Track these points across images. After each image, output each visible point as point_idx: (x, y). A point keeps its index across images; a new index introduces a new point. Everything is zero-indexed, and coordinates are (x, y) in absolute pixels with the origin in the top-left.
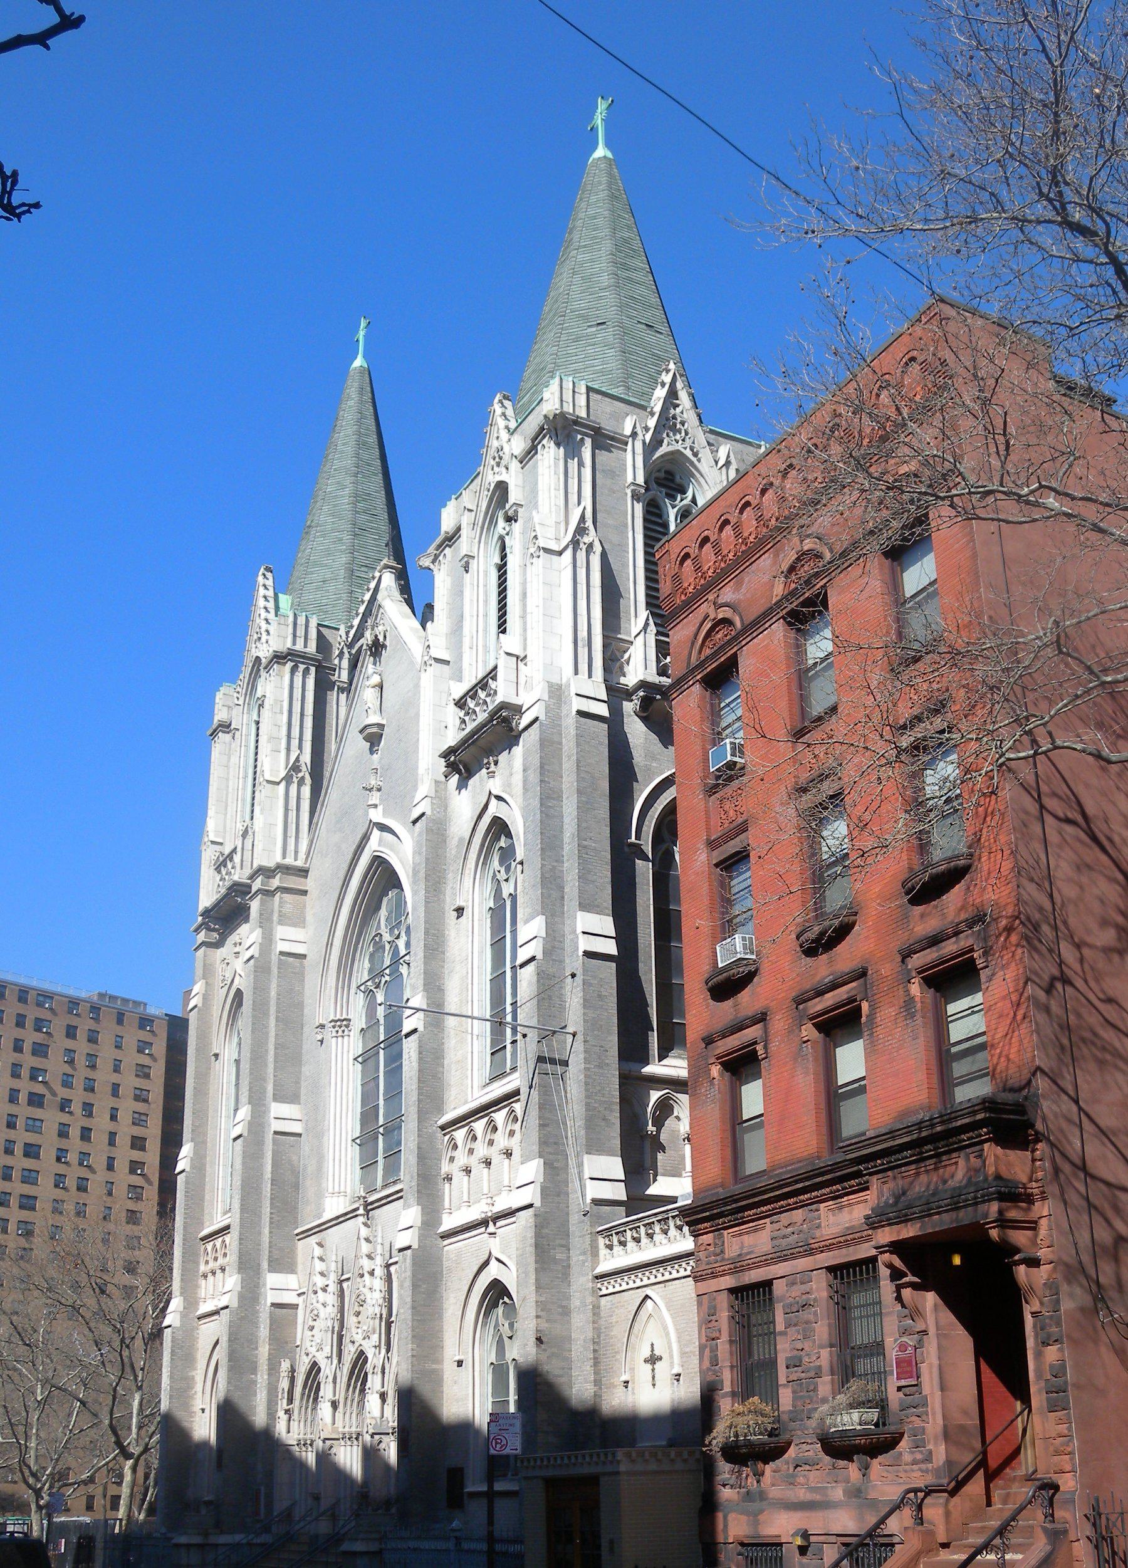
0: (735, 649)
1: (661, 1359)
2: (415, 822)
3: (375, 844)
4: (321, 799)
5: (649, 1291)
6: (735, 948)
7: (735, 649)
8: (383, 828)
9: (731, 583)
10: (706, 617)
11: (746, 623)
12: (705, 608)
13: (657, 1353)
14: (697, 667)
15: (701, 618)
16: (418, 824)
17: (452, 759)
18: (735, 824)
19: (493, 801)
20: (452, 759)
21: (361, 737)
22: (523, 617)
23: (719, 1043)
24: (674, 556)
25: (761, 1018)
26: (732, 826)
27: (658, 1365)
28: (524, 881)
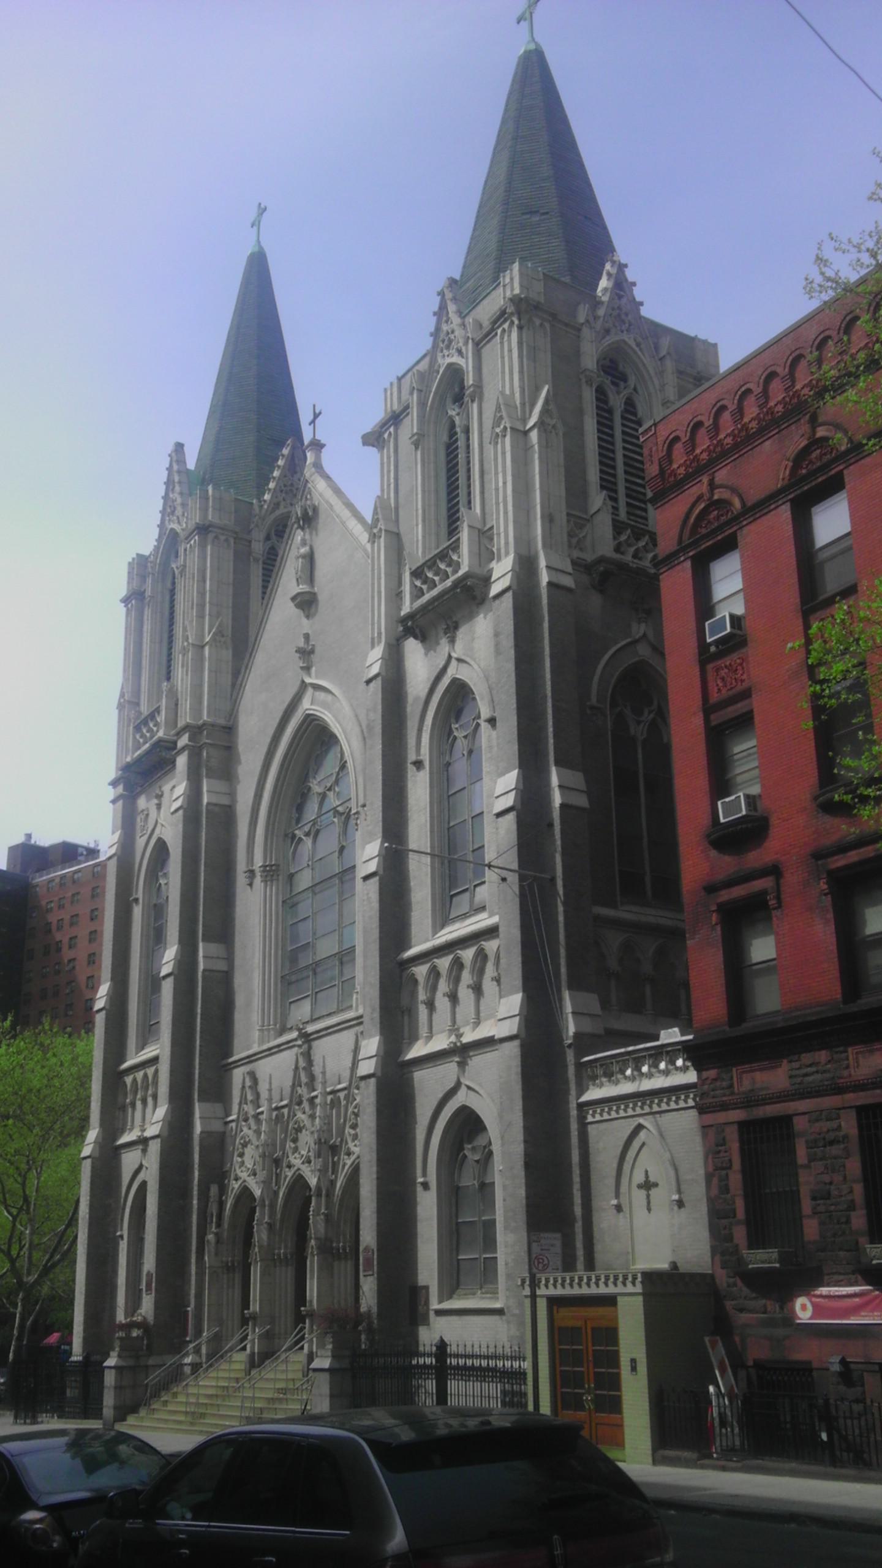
0: (735, 528)
1: (656, 1185)
2: (368, 682)
3: (306, 705)
4: (246, 661)
5: (641, 1121)
6: (732, 808)
7: (735, 528)
8: (317, 687)
9: (729, 467)
10: (700, 498)
11: (749, 504)
12: (701, 487)
13: (652, 1179)
14: (690, 545)
15: (693, 499)
16: (372, 685)
17: (410, 624)
18: (734, 691)
19: (454, 663)
20: (410, 624)
21: (292, 605)
22: (482, 493)
23: (723, 892)
24: (661, 440)
25: (775, 871)
26: (731, 693)
27: (653, 1192)
28: (498, 738)
